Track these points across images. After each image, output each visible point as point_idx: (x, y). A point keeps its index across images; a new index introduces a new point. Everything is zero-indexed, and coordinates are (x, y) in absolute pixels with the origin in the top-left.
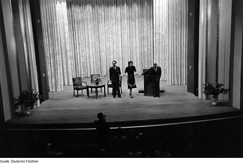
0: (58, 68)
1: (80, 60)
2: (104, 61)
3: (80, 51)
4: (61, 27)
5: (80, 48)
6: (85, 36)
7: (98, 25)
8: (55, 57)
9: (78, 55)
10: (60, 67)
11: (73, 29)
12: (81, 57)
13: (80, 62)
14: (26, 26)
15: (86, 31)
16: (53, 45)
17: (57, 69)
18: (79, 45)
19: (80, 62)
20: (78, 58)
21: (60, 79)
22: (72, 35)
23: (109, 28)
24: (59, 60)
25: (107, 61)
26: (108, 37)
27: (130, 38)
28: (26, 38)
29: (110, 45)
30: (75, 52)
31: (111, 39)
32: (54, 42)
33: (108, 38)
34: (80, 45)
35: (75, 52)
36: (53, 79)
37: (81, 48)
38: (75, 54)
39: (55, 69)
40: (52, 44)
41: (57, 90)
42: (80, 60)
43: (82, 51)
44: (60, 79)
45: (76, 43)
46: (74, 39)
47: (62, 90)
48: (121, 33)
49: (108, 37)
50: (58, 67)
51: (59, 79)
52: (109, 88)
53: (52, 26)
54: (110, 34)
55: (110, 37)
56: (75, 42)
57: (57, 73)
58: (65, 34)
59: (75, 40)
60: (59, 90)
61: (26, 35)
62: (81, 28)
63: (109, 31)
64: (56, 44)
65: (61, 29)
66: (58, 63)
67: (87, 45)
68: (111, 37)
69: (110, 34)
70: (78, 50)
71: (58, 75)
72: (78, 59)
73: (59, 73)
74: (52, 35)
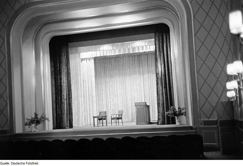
0: (80, 108)
1: (110, 106)
2: (130, 108)
3: (110, 101)
4: (89, 78)
5: (111, 98)
6: (115, 88)
7: (125, 78)
8: (78, 99)
9: (109, 104)
10: (82, 107)
11: (105, 83)
12: (111, 105)
13: (111, 110)
14: (44, 68)
15: (115, 84)
16: (78, 89)
17: (80, 108)
18: (110, 95)
19: (111, 110)
20: (109, 106)
21: (82, 116)
22: (105, 88)
23: (134, 81)
24: (82, 101)
25: (132, 109)
26: (133, 88)
27: (151, 89)
28: (44, 78)
29: (134, 95)
30: (107, 102)
31: (135, 90)
32: (78, 87)
33: (134, 89)
34: (111, 94)
35: (107, 102)
36: (76, 117)
37: (112, 98)
38: (107, 103)
39: (78, 108)
40: (105, 103)
41: (79, 125)
42: (110, 108)
43: (112, 100)
44: (82, 116)
45: (108, 94)
46: (106, 91)
47: (83, 125)
48: (144, 84)
49: (133, 88)
50: (80, 106)
51: (81, 116)
52: (112, 120)
53: (77, 75)
54: (135, 85)
55: (134, 88)
56: (107, 92)
57: (80, 111)
58: (92, 83)
59: (107, 91)
60: (80, 125)
61: (44, 75)
62: (112, 82)
63: (134, 82)
64: (79, 88)
65: (89, 80)
66: (80, 104)
67: (116, 95)
68: (135, 88)
69: (135, 85)
70: (109, 100)
71: (80, 114)
72: (109, 107)
73: (80, 112)
74: (77, 82)
